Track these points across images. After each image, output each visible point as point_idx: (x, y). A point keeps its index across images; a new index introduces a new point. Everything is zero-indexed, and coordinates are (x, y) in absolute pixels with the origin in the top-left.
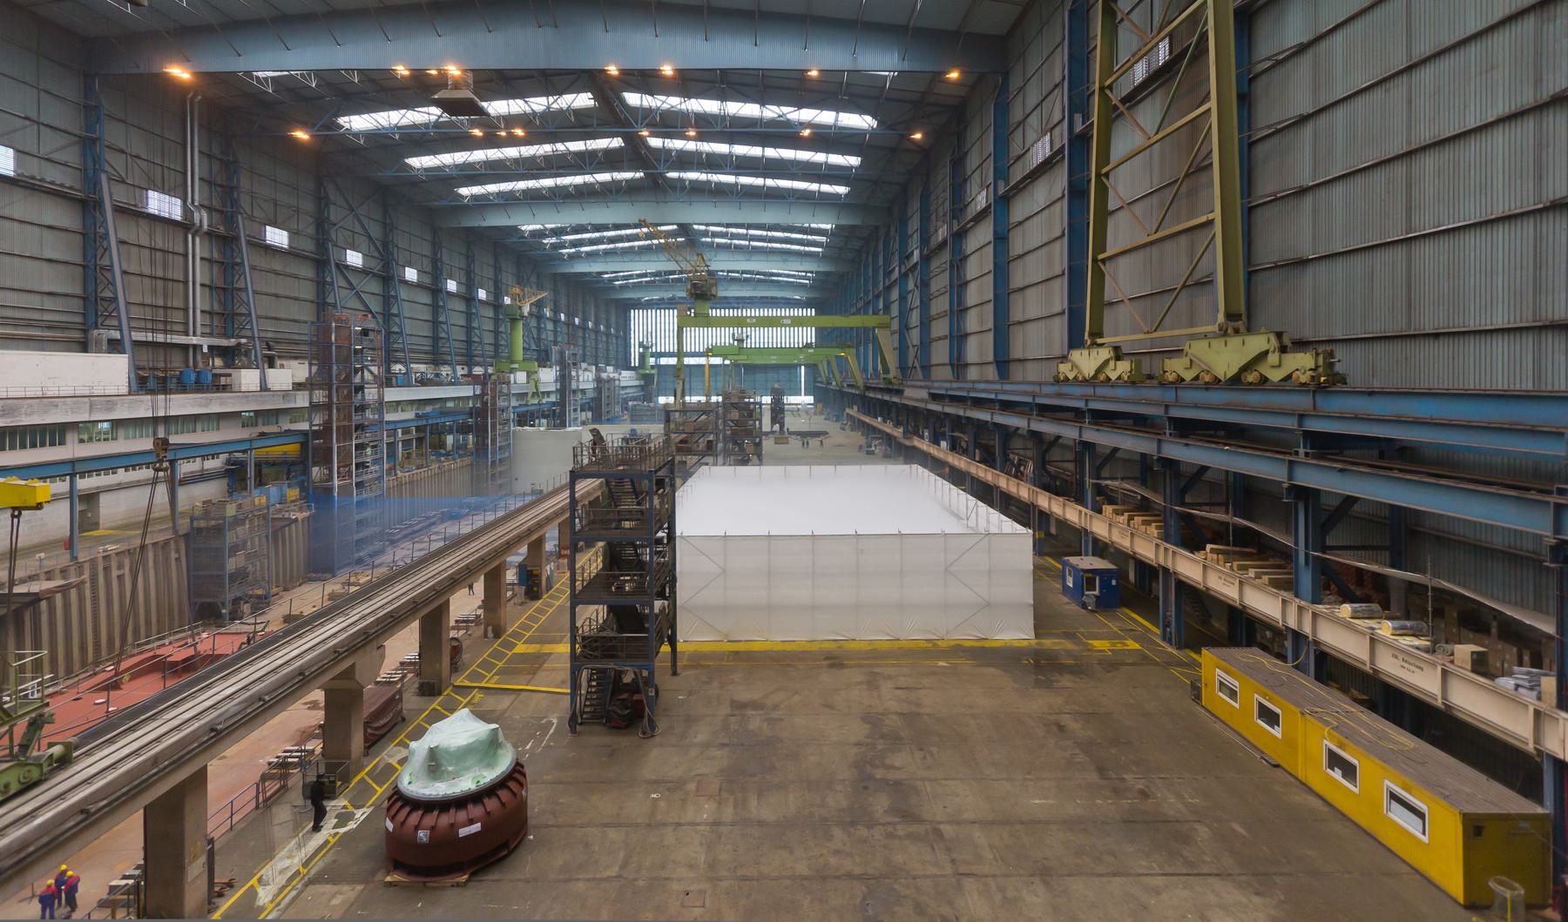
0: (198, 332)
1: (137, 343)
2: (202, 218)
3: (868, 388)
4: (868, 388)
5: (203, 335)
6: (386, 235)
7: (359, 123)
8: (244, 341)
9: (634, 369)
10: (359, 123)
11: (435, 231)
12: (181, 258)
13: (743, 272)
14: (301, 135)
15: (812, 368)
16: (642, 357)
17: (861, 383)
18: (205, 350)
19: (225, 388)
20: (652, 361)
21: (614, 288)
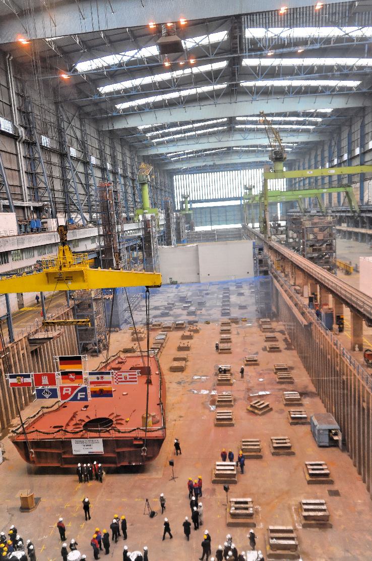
0: (27, 200)
1: (17, 207)
2: (22, 131)
3: (362, 211)
4: (362, 211)
5: (30, 200)
6: (83, 137)
7: (83, 67)
8: (46, 203)
9: (178, 211)
10: (83, 67)
11: (99, 132)
12: (15, 156)
13: (252, 146)
14: (65, 76)
15: (289, 205)
16: (182, 203)
17: (357, 209)
18: (32, 209)
19: (44, 230)
20: (189, 206)
21: (171, 162)
